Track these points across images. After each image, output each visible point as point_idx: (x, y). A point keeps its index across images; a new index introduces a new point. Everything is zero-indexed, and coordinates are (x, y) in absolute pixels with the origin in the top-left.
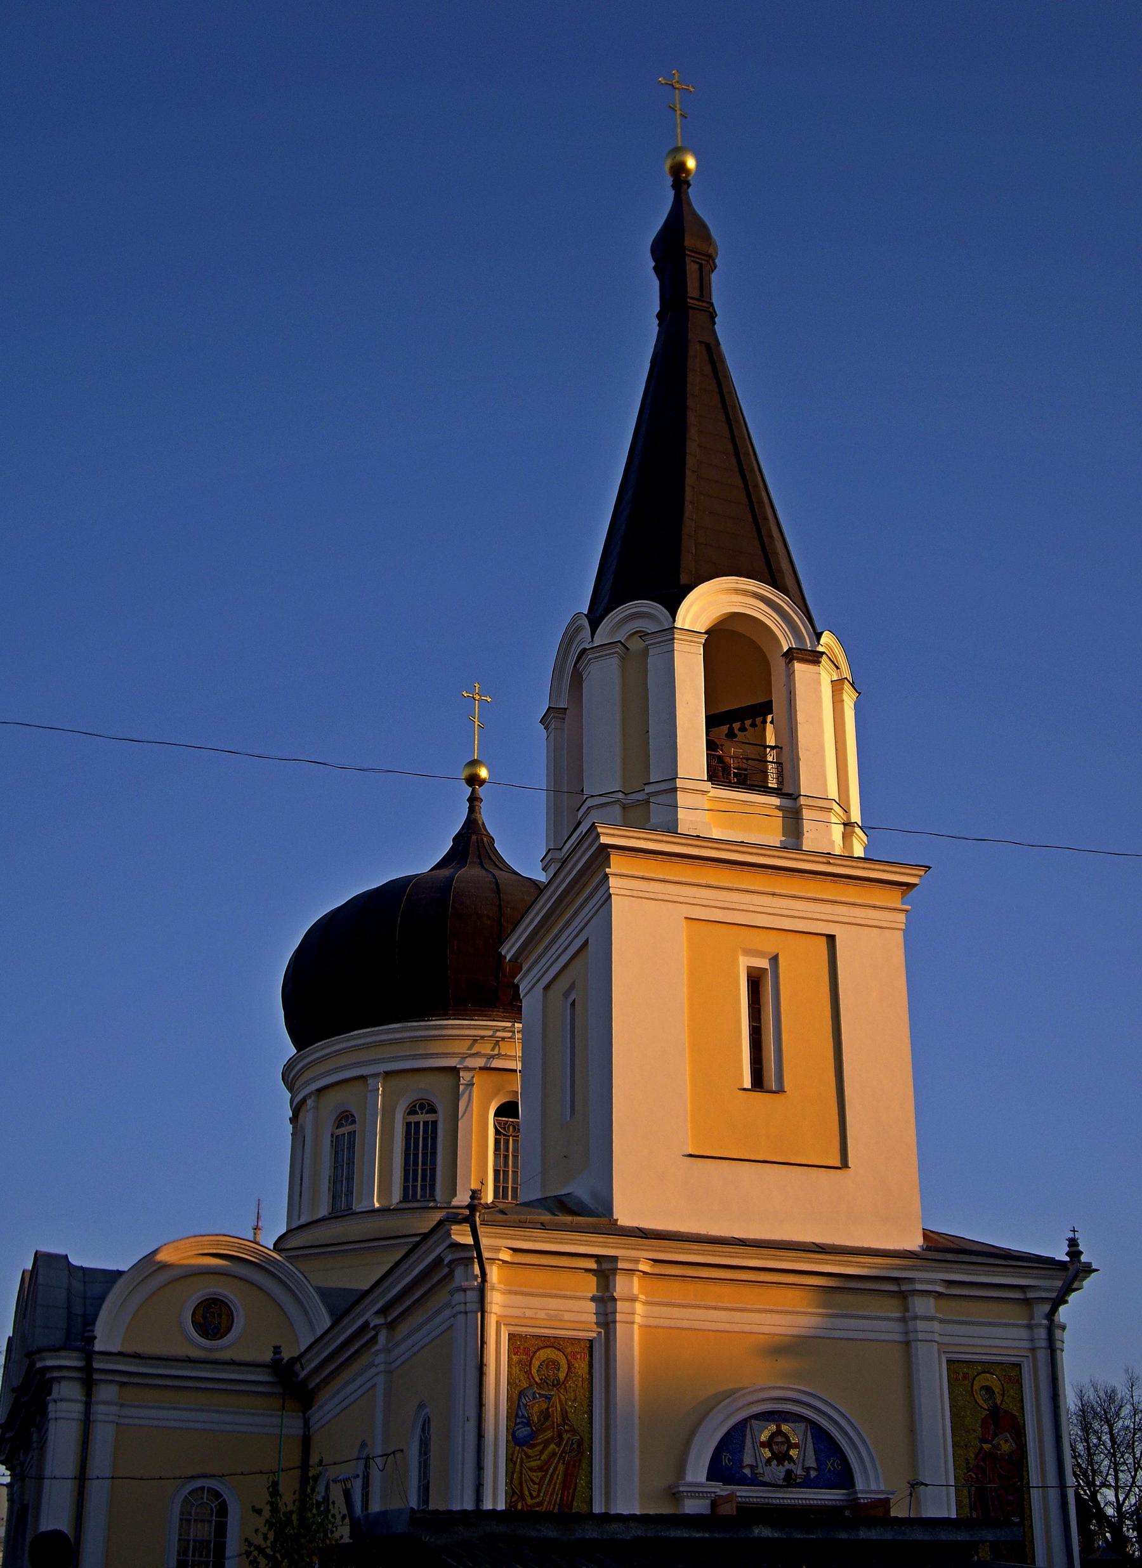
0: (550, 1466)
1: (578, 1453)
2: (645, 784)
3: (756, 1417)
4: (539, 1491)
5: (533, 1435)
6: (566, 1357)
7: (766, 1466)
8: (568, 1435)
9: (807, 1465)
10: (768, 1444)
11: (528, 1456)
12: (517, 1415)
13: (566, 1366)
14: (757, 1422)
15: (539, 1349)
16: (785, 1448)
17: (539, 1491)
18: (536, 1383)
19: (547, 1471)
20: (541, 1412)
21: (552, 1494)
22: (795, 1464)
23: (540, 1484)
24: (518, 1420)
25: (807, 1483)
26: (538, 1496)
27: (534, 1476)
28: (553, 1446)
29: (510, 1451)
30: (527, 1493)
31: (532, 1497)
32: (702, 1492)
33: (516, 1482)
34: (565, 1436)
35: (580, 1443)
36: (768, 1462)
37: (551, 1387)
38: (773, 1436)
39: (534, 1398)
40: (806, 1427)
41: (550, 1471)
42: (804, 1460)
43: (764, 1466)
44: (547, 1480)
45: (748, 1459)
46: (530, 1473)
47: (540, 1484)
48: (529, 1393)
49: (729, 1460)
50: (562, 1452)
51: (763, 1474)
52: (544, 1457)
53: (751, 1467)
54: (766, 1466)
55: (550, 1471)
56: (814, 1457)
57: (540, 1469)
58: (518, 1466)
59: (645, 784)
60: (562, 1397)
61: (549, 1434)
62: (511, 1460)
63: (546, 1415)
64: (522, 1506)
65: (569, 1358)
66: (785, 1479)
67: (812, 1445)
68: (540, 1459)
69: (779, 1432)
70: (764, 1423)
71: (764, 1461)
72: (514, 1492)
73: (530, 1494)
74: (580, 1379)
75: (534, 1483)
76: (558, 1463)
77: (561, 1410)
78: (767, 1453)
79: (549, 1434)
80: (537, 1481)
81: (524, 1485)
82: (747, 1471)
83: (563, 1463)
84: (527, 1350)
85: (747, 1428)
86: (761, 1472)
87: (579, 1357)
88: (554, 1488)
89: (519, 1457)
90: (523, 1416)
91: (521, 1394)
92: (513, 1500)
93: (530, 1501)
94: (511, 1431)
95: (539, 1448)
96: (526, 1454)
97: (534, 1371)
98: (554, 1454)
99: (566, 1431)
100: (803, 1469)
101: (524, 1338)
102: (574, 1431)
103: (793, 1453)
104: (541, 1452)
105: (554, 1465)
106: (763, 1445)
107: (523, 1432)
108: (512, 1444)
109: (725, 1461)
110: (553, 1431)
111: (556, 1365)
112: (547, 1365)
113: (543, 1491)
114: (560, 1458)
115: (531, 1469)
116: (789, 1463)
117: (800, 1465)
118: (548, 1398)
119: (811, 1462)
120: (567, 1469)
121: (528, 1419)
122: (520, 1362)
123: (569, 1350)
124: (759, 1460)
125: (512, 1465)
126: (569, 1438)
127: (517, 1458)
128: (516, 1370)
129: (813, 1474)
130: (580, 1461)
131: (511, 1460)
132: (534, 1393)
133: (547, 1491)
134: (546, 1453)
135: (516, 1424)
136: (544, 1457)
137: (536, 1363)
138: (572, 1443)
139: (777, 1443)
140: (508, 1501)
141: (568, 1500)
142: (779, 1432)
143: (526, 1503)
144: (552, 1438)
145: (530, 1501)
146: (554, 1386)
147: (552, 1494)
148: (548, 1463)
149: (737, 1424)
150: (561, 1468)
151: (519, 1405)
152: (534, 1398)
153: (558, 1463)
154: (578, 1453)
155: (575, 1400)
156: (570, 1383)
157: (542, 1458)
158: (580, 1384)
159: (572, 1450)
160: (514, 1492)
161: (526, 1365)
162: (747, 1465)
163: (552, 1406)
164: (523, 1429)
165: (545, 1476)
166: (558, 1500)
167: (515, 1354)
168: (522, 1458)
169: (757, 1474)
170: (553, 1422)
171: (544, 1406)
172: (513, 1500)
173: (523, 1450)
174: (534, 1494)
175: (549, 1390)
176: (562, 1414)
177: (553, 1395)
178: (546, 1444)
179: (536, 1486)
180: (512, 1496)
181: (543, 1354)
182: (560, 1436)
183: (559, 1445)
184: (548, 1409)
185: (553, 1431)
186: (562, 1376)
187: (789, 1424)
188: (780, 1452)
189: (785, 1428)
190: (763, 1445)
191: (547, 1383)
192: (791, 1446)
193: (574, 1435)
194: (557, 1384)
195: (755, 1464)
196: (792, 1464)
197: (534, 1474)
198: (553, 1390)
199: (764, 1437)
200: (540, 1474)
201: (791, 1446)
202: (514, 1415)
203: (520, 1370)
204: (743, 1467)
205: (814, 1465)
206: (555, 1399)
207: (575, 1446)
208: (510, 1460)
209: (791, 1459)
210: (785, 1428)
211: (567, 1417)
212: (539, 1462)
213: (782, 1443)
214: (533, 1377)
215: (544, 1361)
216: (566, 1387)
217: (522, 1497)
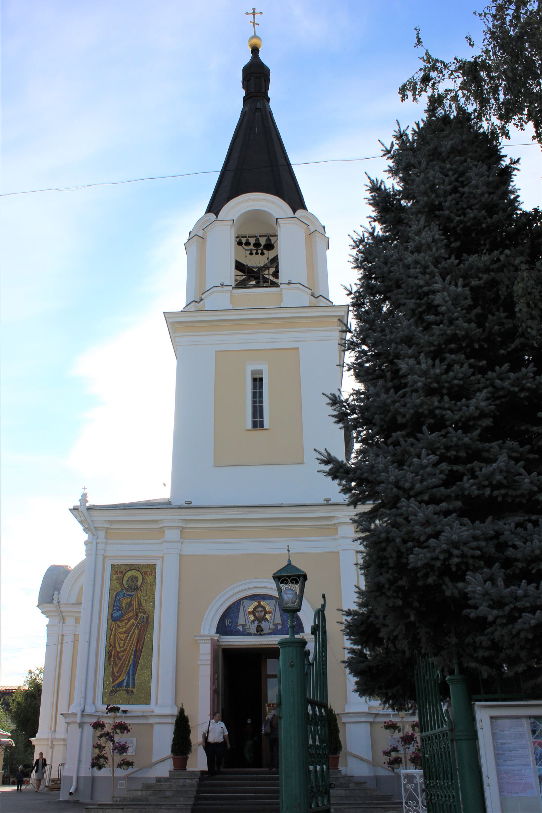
0: (131, 631)
1: (147, 623)
2: (202, 294)
3: (246, 598)
4: (124, 644)
5: (122, 616)
6: (142, 574)
7: (251, 624)
8: (142, 614)
9: (276, 622)
10: (253, 612)
11: (119, 626)
12: (114, 606)
13: (142, 579)
14: (246, 601)
15: (127, 571)
16: (263, 613)
17: (124, 644)
18: (125, 588)
19: (129, 634)
20: (127, 603)
21: (131, 646)
22: (269, 622)
23: (125, 640)
24: (115, 608)
25: (275, 632)
26: (124, 646)
27: (123, 636)
28: (132, 620)
29: (110, 624)
30: (117, 645)
31: (120, 647)
32: (204, 640)
33: (112, 640)
34: (140, 615)
35: (148, 618)
36: (253, 622)
37: (133, 590)
38: (255, 609)
39: (124, 596)
40: (276, 602)
41: (131, 633)
42: (274, 620)
43: (250, 624)
44: (129, 638)
45: (241, 621)
46: (120, 635)
47: (125, 640)
48: (121, 594)
49: (230, 622)
50: (138, 623)
51: (250, 628)
52: (128, 626)
53: (243, 626)
54: (251, 624)
55: (131, 633)
56: (280, 618)
57: (125, 632)
58: (113, 631)
59: (202, 294)
60: (139, 595)
61: (131, 614)
62: (110, 629)
63: (130, 604)
64: (115, 652)
65: (143, 574)
66: (257, 631)
67: (279, 611)
68: (125, 628)
69: (259, 605)
70: (251, 602)
71: (250, 621)
72: (111, 645)
73: (119, 646)
74: (149, 585)
75: (122, 640)
76: (135, 629)
77: (138, 602)
78: (252, 617)
79: (131, 614)
80: (123, 638)
81: (116, 641)
82: (240, 628)
83: (138, 629)
84: (121, 572)
85: (240, 604)
86: (249, 627)
87: (149, 573)
88: (133, 642)
89: (114, 627)
90: (117, 606)
91: (117, 595)
92: (110, 649)
93: (119, 649)
94: (110, 613)
95: (126, 621)
96: (118, 625)
97: (124, 582)
98: (133, 624)
99: (141, 612)
100: (273, 624)
101: (120, 566)
102: (145, 612)
103: (268, 616)
104: (126, 624)
105: (133, 630)
106: (250, 613)
107: (117, 614)
108: (111, 621)
109: (227, 622)
110: (133, 613)
111: (136, 579)
112: (132, 580)
113: (126, 644)
114: (135, 628)
115: (120, 633)
116: (265, 622)
117: (272, 623)
118: (131, 596)
119: (278, 620)
120: (140, 631)
121: (120, 607)
122: (117, 579)
123: (144, 570)
124: (247, 621)
125: (110, 631)
126: (142, 616)
127: (113, 627)
128: (115, 582)
129: (279, 627)
130: (147, 627)
131: (110, 629)
132: (124, 594)
133: (128, 644)
134: (129, 624)
135: (114, 610)
136: (128, 626)
137: (125, 579)
138: (143, 618)
139: (258, 612)
140: (107, 650)
141: (139, 648)
142: (259, 605)
143: (117, 650)
144: (133, 616)
145: (119, 649)
146: (134, 589)
147: (131, 646)
148: (130, 629)
149: (235, 603)
150: (137, 631)
151: (115, 600)
152: (124, 596)
153: (135, 629)
154: (147, 623)
155: (146, 596)
156: (143, 588)
157: (127, 627)
158: (149, 587)
159: (142, 622)
160: (111, 645)
161: (120, 580)
162: (240, 625)
163: (133, 600)
164: (117, 613)
165: (127, 636)
166: (134, 648)
167: (114, 575)
168: (116, 628)
169: (246, 629)
170: (133, 607)
171: (129, 600)
172: (110, 649)
173: (116, 623)
174: (122, 646)
175: (132, 591)
176: (139, 604)
177: (134, 594)
178: (129, 619)
179: (123, 642)
180: (110, 647)
181: (129, 574)
182: (137, 615)
183: (136, 620)
184: (131, 601)
185: (133, 613)
186: (139, 583)
187: (265, 601)
188: (260, 616)
189: (263, 603)
190: (250, 613)
191: (131, 588)
192: (266, 613)
193: (145, 614)
194: (137, 588)
195: (245, 623)
196: (267, 622)
197: (122, 635)
198: (134, 591)
199: (251, 609)
200: (125, 635)
201: (266, 613)
202: (113, 605)
203: (117, 582)
204: (238, 626)
205: (280, 622)
206: (135, 597)
207: (145, 620)
208: (109, 629)
209: (266, 620)
210: (263, 603)
211: (141, 605)
212: (124, 629)
213: (261, 611)
214: (123, 585)
215: (130, 577)
216: (141, 590)
217: (115, 647)
